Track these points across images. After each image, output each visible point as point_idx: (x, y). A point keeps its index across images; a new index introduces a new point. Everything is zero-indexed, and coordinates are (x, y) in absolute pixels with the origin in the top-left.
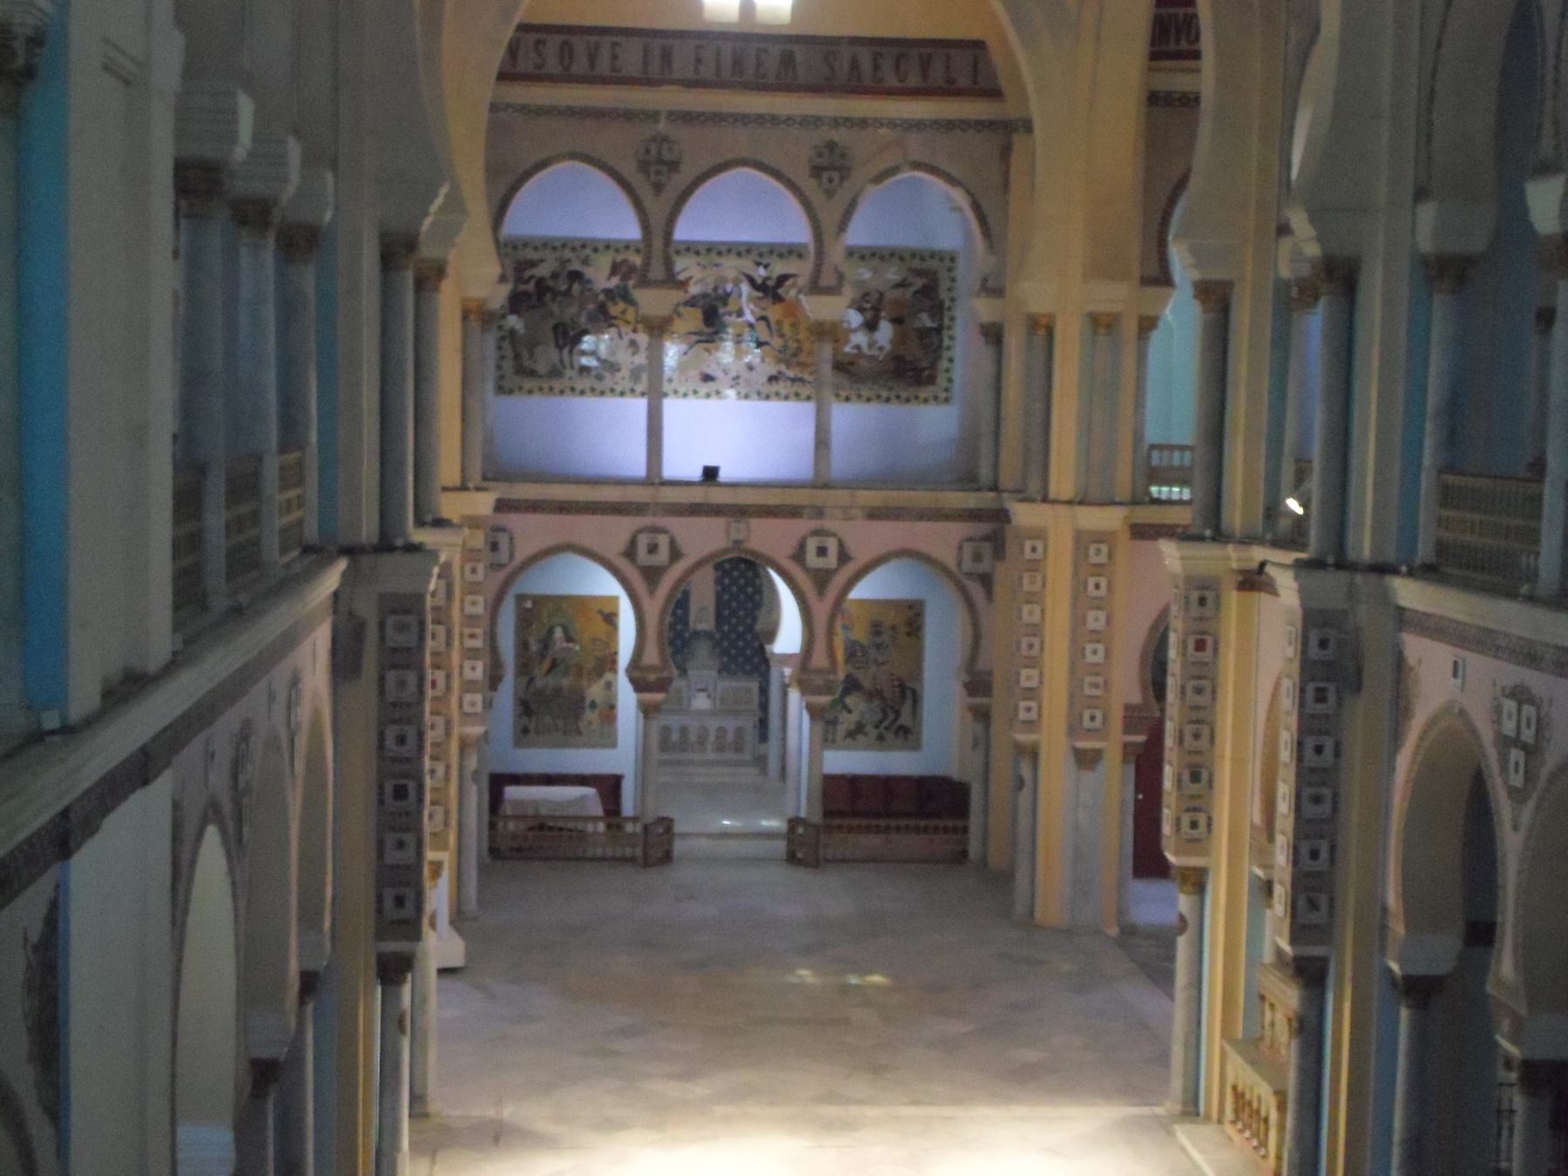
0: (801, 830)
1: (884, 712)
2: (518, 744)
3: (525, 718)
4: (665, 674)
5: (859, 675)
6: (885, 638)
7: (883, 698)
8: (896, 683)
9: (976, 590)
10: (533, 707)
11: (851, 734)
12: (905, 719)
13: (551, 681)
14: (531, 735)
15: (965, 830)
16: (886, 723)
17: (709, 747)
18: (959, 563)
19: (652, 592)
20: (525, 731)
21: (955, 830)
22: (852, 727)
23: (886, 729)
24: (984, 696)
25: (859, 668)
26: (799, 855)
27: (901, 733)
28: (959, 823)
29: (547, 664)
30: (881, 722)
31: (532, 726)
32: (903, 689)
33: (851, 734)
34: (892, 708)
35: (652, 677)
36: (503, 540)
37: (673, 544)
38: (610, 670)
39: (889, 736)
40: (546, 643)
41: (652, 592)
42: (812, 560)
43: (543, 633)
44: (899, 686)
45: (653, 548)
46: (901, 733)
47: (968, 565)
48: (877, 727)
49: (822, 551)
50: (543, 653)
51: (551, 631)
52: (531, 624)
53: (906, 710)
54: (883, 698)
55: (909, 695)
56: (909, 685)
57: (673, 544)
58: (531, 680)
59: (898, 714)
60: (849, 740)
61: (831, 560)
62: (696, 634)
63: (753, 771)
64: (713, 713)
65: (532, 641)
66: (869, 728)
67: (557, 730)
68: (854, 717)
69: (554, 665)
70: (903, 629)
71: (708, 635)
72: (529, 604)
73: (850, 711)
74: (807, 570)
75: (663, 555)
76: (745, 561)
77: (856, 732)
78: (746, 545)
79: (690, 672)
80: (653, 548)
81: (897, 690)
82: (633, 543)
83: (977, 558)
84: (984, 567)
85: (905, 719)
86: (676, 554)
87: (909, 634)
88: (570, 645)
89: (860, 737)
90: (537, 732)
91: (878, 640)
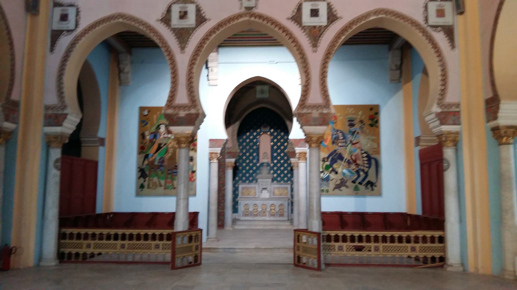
0: (304, 239)
1: (358, 172)
2: (138, 195)
3: (142, 180)
4: (193, 111)
5: (340, 150)
6: (357, 127)
7: (357, 165)
8: (365, 155)
9: (440, 38)
10: (147, 172)
11: (338, 187)
12: (371, 177)
13: (157, 156)
14: (145, 190)
15: (442, 240)
16: (360, 180)
17: (267, 214)
18: (426, 19)
19: (183, 48)
20: (142, 186)
21: (433, 239)
22: (339, 182)
23: (360, 183)
24: (454, 124)
25: (341, 146)
26: (304, 260)
27: (369, 186)
28: (437, 234)
29: (155, 147)
30: (357, 179)
31: (146, 184)
32: (369, 158)
33: (338, 187)
34: (363, 170)
35: (182, 114)
36: (71, 13)
37: (198, 10)
38: (193, 149)
39: (362, 188)
40: (155, 135)
41: (183, 48)
42: (307, 19)
43: (153, 129)
44: (366, 157)
45: (183, 15)
46: (369, 186)
47: (433, 20)
48: (354, 182)
49: (315, 13)
50: (152, 142)
51: (158, 128)
52: (147, 124)
53: (372, 172)
54: (357, 165)
55: (373, 162)
56: (372, 156)
57: (198, 10)
58: (147, 156)
59: (366, 174)
60: (336, 190)
61: (322, 20)
62: (262, 164)
63: (288, 223)
64: (270, 199)
65: (147, 133)
66: (349, 183)
67: (161, 186)
68: (339, 177)
69: (159, 148)
70: (368, 122)
71: (268, 165)
72: (146, 113)
73: (337, 173)
74: (304, 28)
75: (191, 20)
76: (292, 170)
77: (341, 185)
78: (255, 11)
79: (259, 180)
80: (183, 15)
81: (366, 159)
82: (169, 11)
83: (441, 13)
84: (448, 19)
85: (371, 177)
86: (201, 19)
87: (371, 125)
88: (170, 136)
89: (343, 188)
90: (149, 187)
91: (353, 129)
